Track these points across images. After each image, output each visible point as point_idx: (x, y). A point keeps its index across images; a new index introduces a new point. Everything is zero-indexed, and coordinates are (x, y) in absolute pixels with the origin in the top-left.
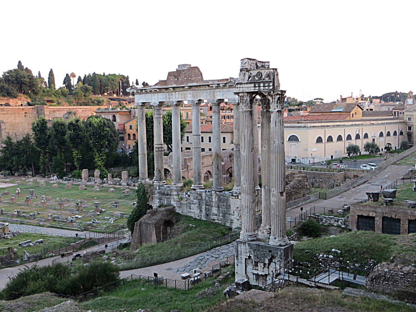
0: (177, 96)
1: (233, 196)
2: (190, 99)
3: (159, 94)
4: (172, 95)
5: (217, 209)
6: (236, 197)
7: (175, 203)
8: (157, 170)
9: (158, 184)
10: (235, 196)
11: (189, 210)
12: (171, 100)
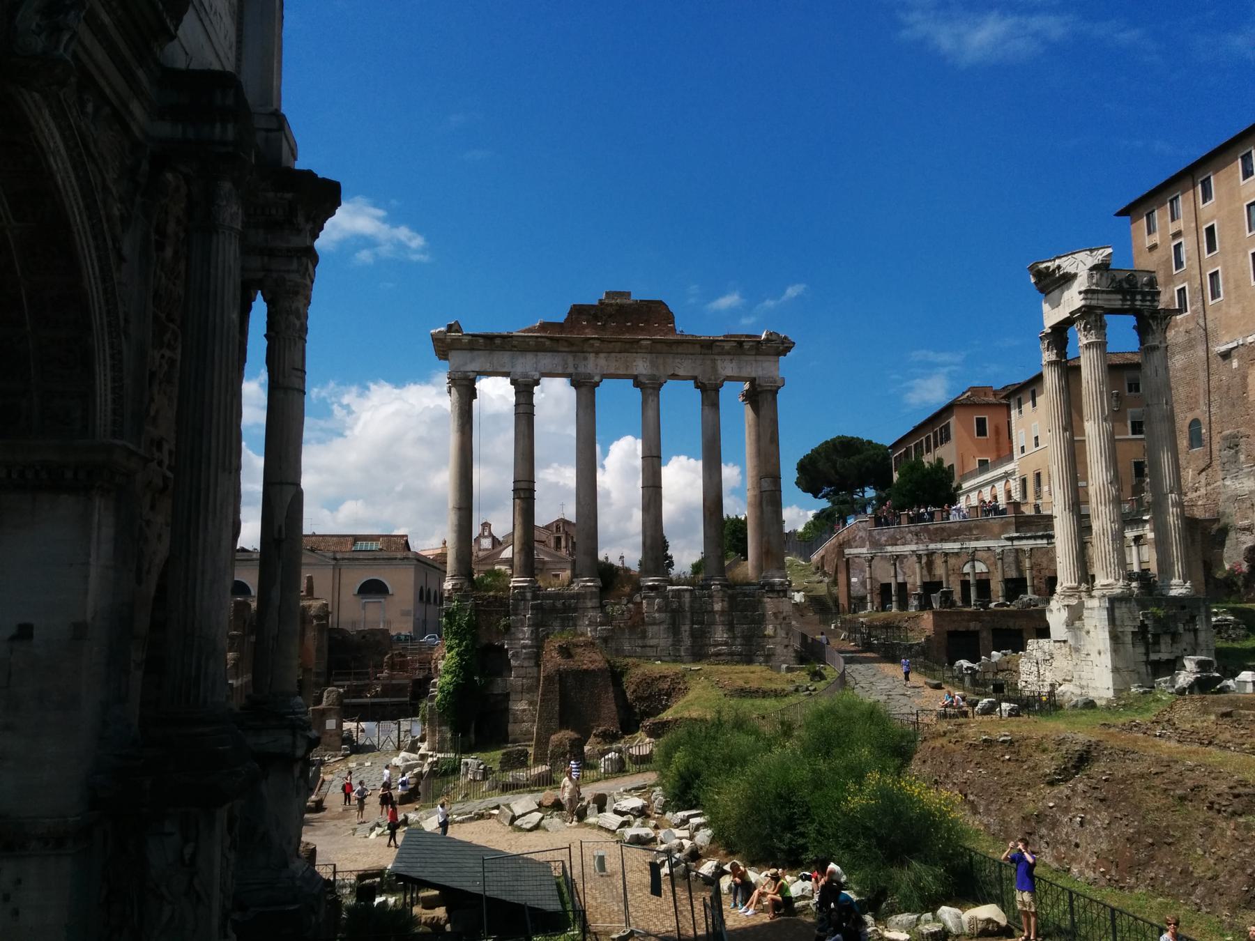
4: (585, 359)
10: (779, 592)
11: (640, 642)
12: (581, 370)
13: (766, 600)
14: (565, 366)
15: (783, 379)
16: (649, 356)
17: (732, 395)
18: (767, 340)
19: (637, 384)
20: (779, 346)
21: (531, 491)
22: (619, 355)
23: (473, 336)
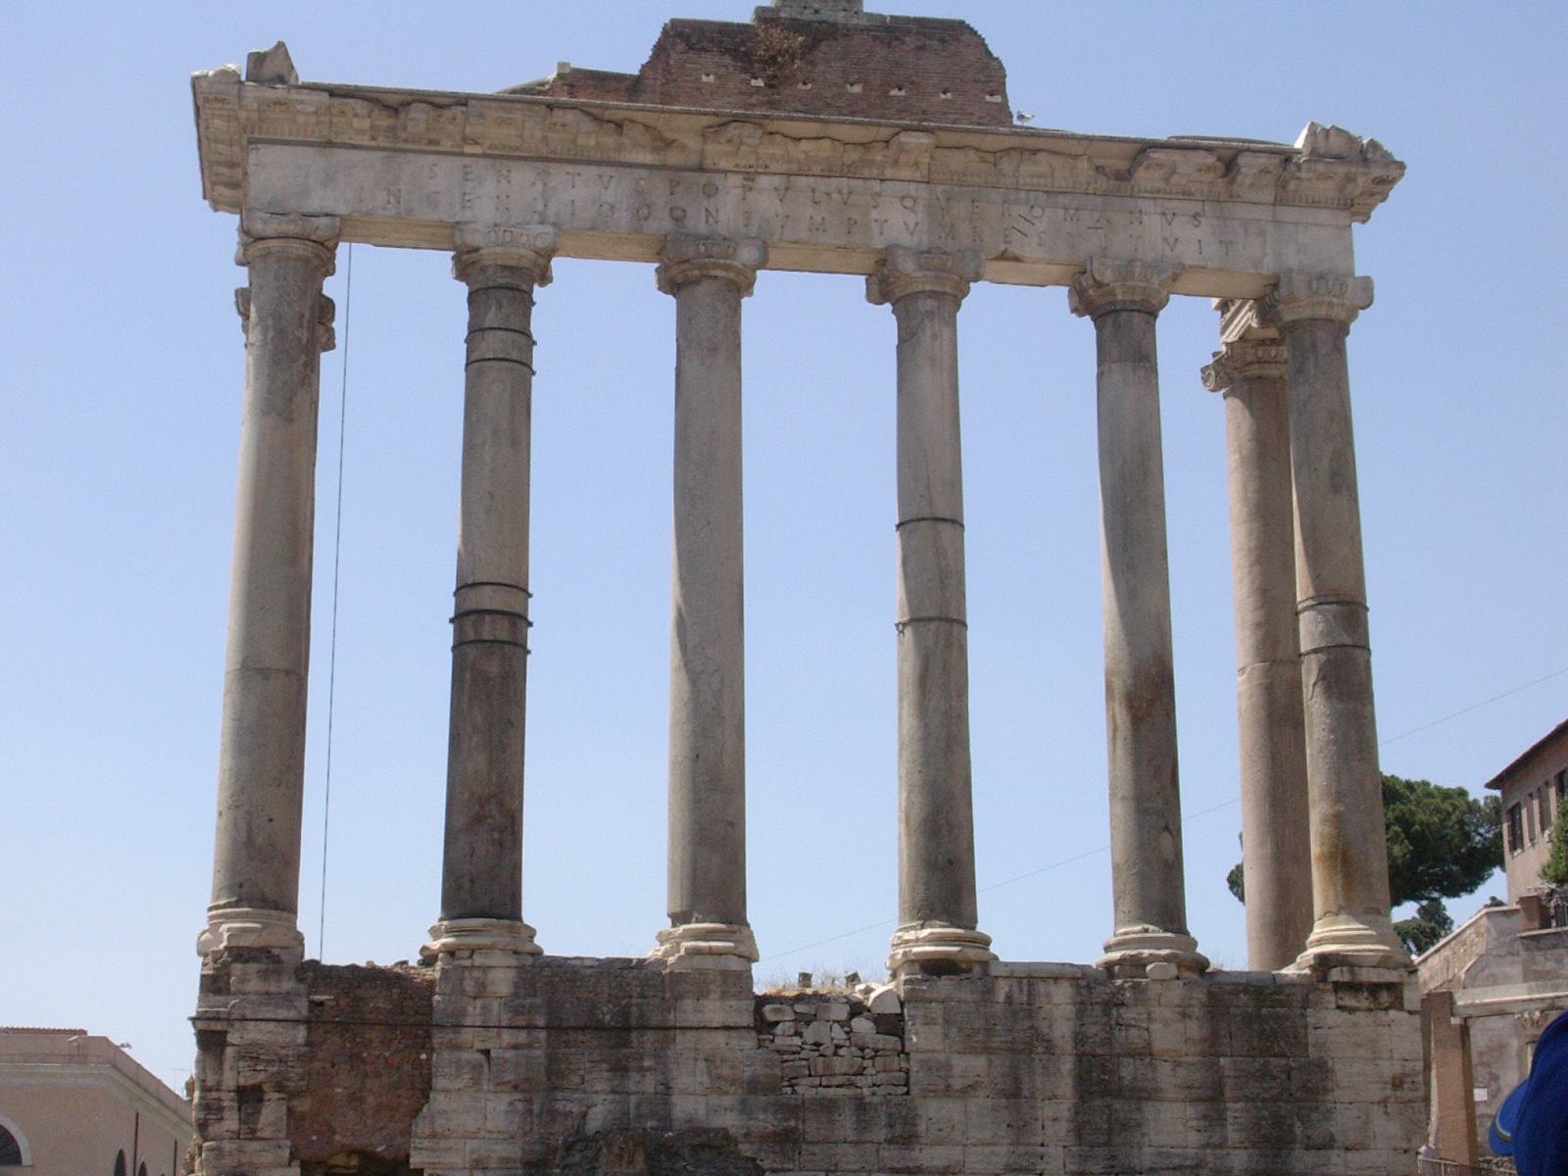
0: (766, 200)
1: (1354, 987)
2: (906, 240)
3: (553, 167)
4: (711, 191)
5: (1191, 1111)
6: (1385, 998)
7: (727, 1101)
8: (493, 808)
9: (504, 940)
10: (1375, 989)
12: (697, 224)
13: (1333, 1017)
14: (642, 209)
15: (1367, 285)
16: (921, 192)
17: (1191, 332)
18: (1315, 154)
19: (882, 289)
20: (1356, 173)
21: (519, 620)
22: (823, 185)
23: (334, 92)
